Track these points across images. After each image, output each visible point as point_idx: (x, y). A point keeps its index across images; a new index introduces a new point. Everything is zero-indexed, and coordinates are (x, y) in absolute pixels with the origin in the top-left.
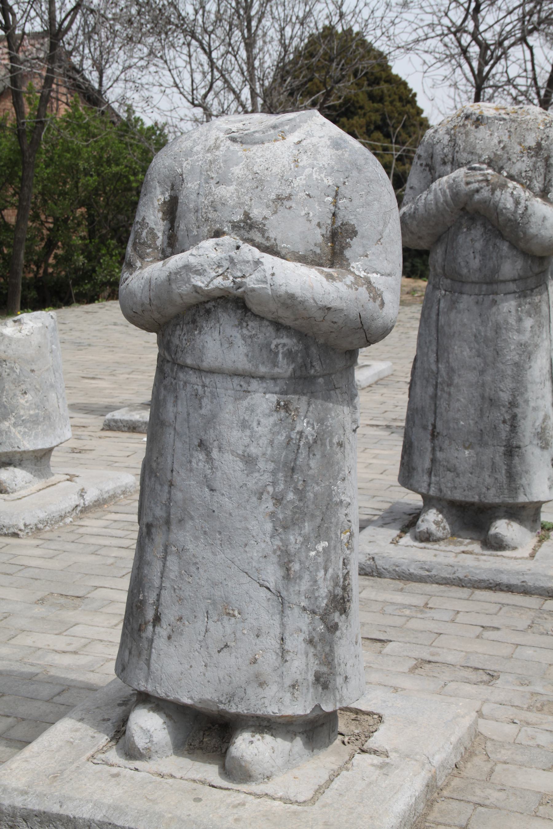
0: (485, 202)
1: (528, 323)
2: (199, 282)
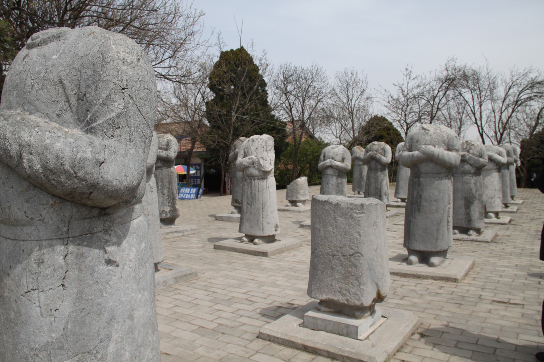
0: (375, 157)
1: (382, 176)
2: (327, 164)
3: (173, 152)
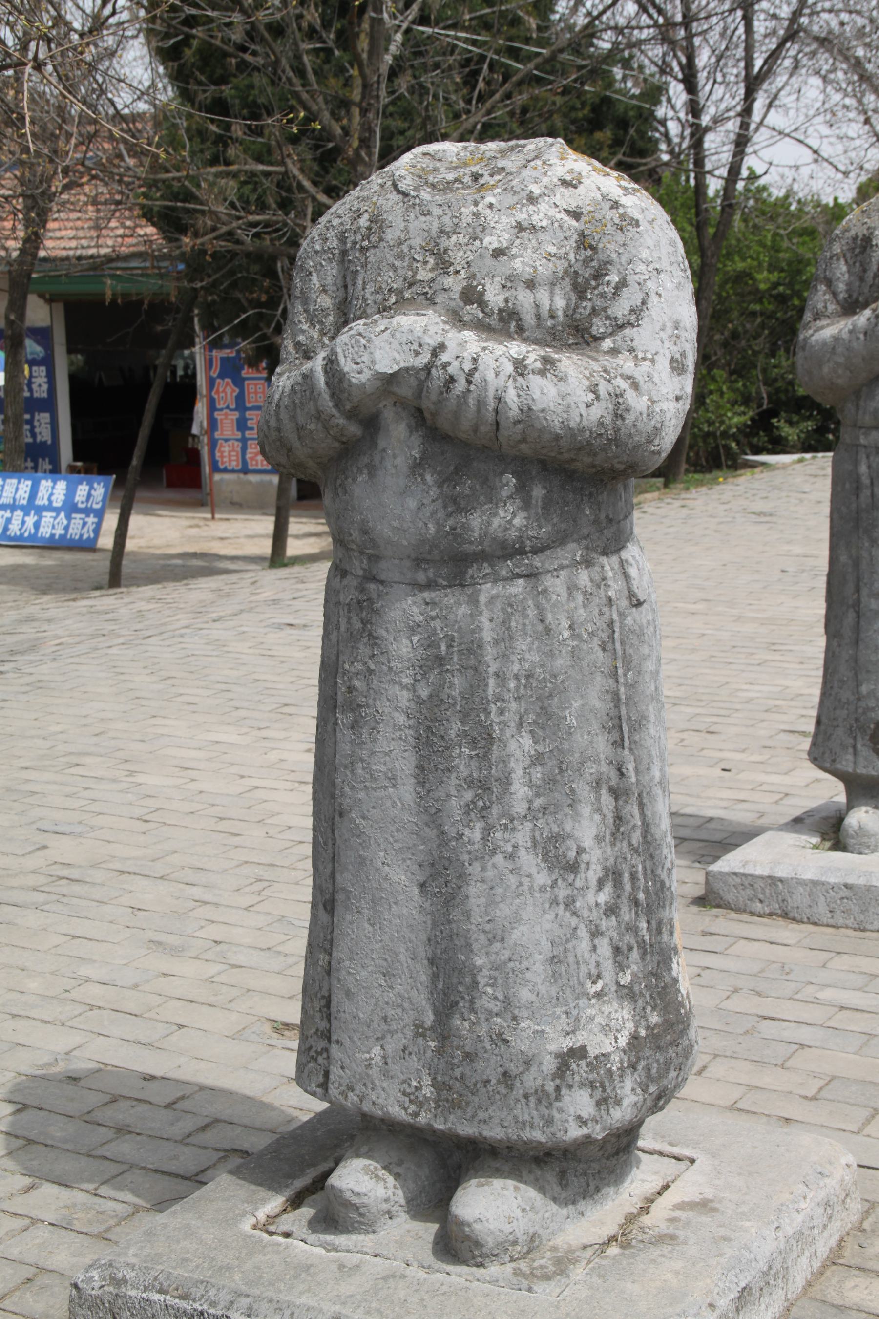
3: (663, 364)
